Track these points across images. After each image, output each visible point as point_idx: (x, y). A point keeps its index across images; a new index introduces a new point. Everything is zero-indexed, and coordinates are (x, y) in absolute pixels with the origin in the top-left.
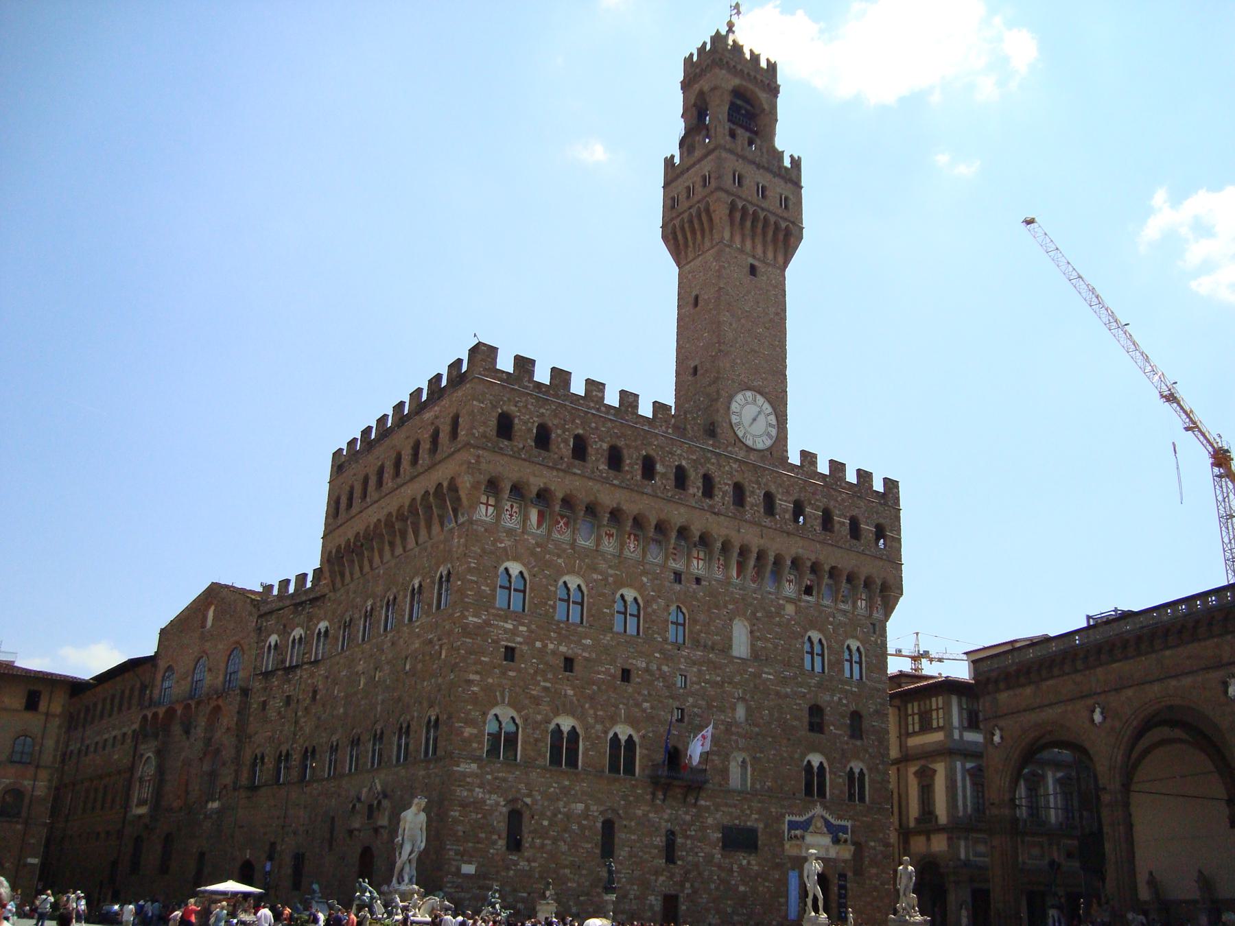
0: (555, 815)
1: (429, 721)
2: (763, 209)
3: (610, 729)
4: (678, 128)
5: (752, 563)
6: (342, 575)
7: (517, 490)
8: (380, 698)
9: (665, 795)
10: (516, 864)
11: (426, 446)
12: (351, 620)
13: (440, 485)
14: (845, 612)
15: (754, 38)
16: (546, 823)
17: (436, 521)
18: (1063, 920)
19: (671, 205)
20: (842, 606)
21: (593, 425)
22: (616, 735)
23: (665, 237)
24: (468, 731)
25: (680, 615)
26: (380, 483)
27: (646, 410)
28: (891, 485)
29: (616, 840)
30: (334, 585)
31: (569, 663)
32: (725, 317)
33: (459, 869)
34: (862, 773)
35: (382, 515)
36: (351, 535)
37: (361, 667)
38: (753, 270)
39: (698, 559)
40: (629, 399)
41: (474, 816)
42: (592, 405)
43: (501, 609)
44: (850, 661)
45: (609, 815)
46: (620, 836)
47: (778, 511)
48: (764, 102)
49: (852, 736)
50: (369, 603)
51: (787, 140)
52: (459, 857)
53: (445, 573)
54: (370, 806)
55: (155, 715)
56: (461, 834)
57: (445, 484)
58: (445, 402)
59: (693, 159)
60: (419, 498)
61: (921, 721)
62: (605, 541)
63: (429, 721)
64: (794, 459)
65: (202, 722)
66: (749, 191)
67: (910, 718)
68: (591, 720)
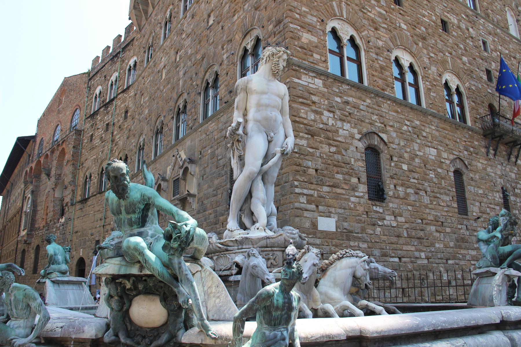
0: (413, 159)
3: (443, 73)
6: (146, 12)
8: (181, 73)
9: (495, 150)
16: (405, 167)
24: (306, 37)
29: (467, 195)
30: (139, 25)
33: (315, 225)
41: (326, 148)
46: (470, 189)
52: (313, 207)
54: (176, 182)
55: (31, 168)
56: (312, 172)
65: (55, 163)
68: (426, 60)
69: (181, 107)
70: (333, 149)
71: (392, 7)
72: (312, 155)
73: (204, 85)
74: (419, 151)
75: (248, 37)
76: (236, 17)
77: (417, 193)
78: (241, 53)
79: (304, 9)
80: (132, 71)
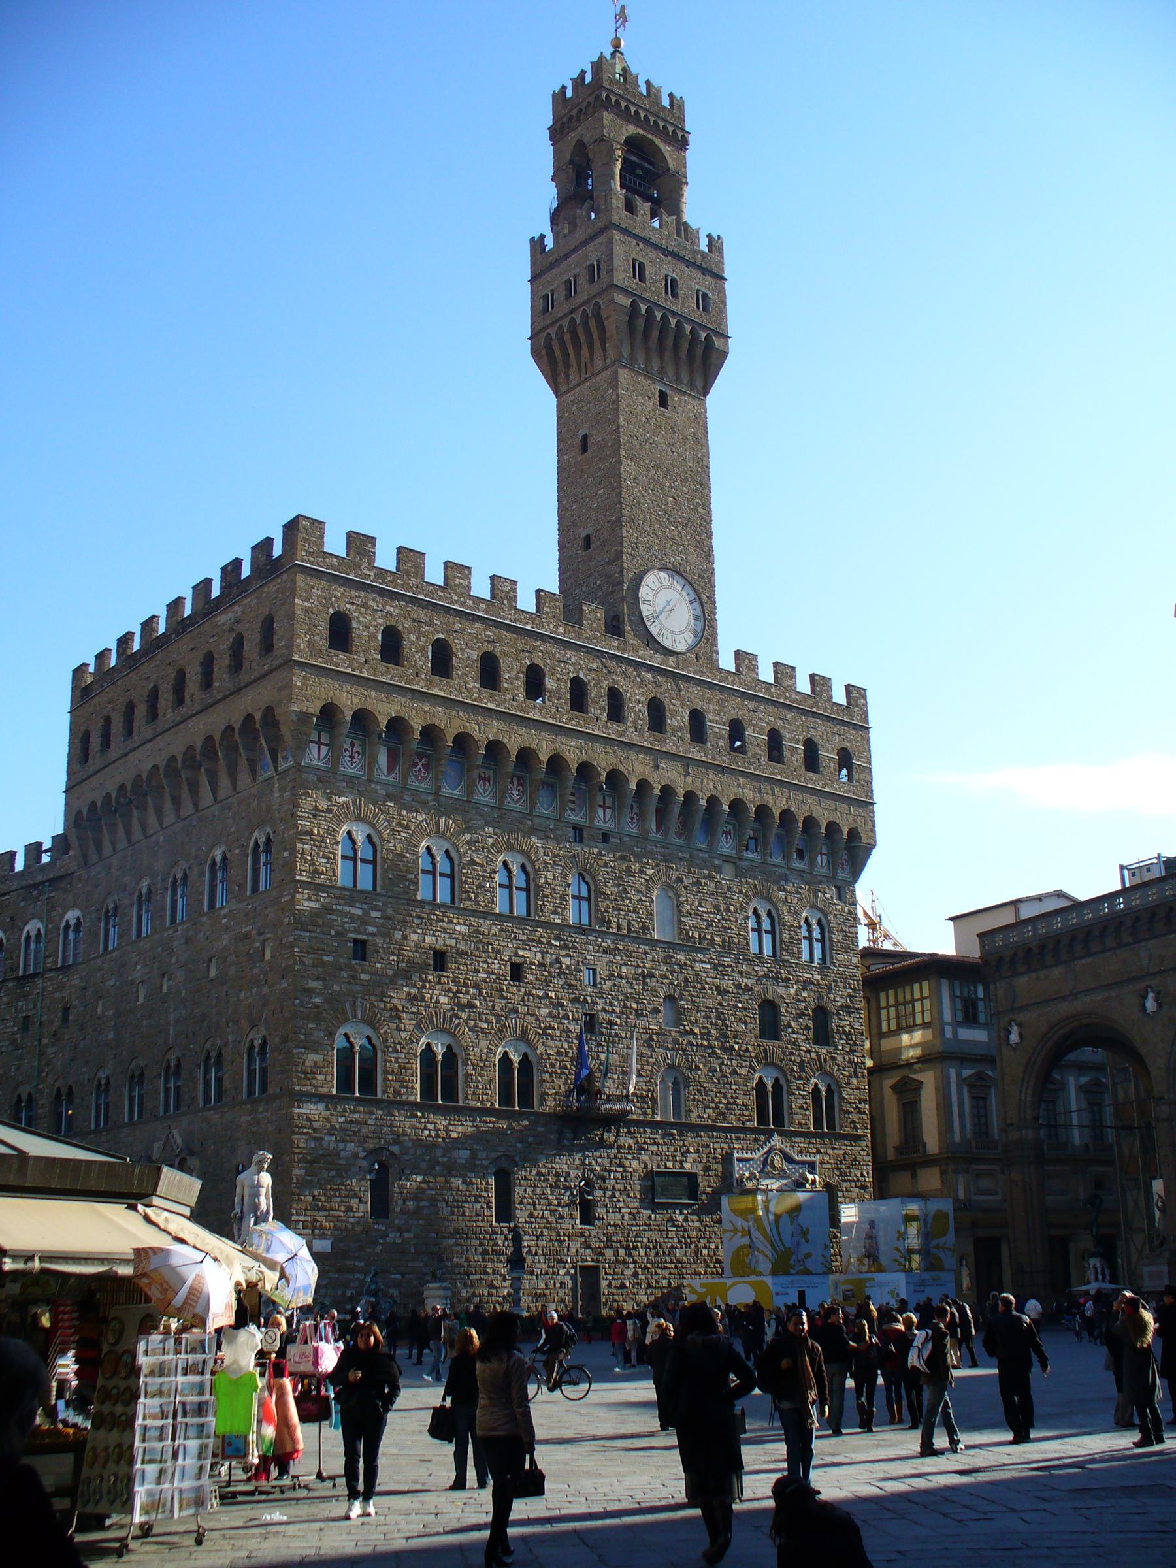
0: (433, 1168)
1: (252, 1046)
2: (674, 313)
4: (547, 195)
5: (677, 810)
6: (99, 845)
7: (362, 718)
8: (172, 1017)
10: (385, 1236)
11: (222, 663)
12: (116, 908)
13: (249, 718)
14: (800, 872)
15: (653, 66)
17: (243, 764)
18: (1107, 1272)
19: (542, 306)
20: (797, 864)
21: (458, 626)
22: (506, 1053)
23: (535, 353)
25: (584, 887)
26: (153, 714)
27: (526, 602)
28: (855, 694)
30: (85, 856)
31: (440, 959)
32: (627, 468)
34: (829, 1090)
35: (161, 760)
36: (111, 788)
37: (138, 972)
38: (663, 400)
39: (604, 807)
40: (503, 588)
41: (325, 1174)
42: (455, 597)
43: (347, 889)
44: (810, 939)
45: (503, 1164)
47: (710, 738)
48: (667, 156)
49: (817, 1041)
50: (144, 885)
51: (701, 208)
53: (262, 840)
57: (258, 716)
58: (251, 601)
59: (573, 243)
60: (217, 736)
61: (898, 1017)
62: (480, 787)
63: (252, 1046)
64: (727, 662)
66: (655, 290)
67: (884, 1013)
69: (173, 1064)
70: (333, 1173)
71: (430, 977)
72: (311, 1181)
73: (204, 1054)
74: (444, 1156)
75: (255, 1029)
76: (242, 995)
77: (432, 1205)
78: (247, 1045)
79: (311, 1026)
80: (71, 935)
